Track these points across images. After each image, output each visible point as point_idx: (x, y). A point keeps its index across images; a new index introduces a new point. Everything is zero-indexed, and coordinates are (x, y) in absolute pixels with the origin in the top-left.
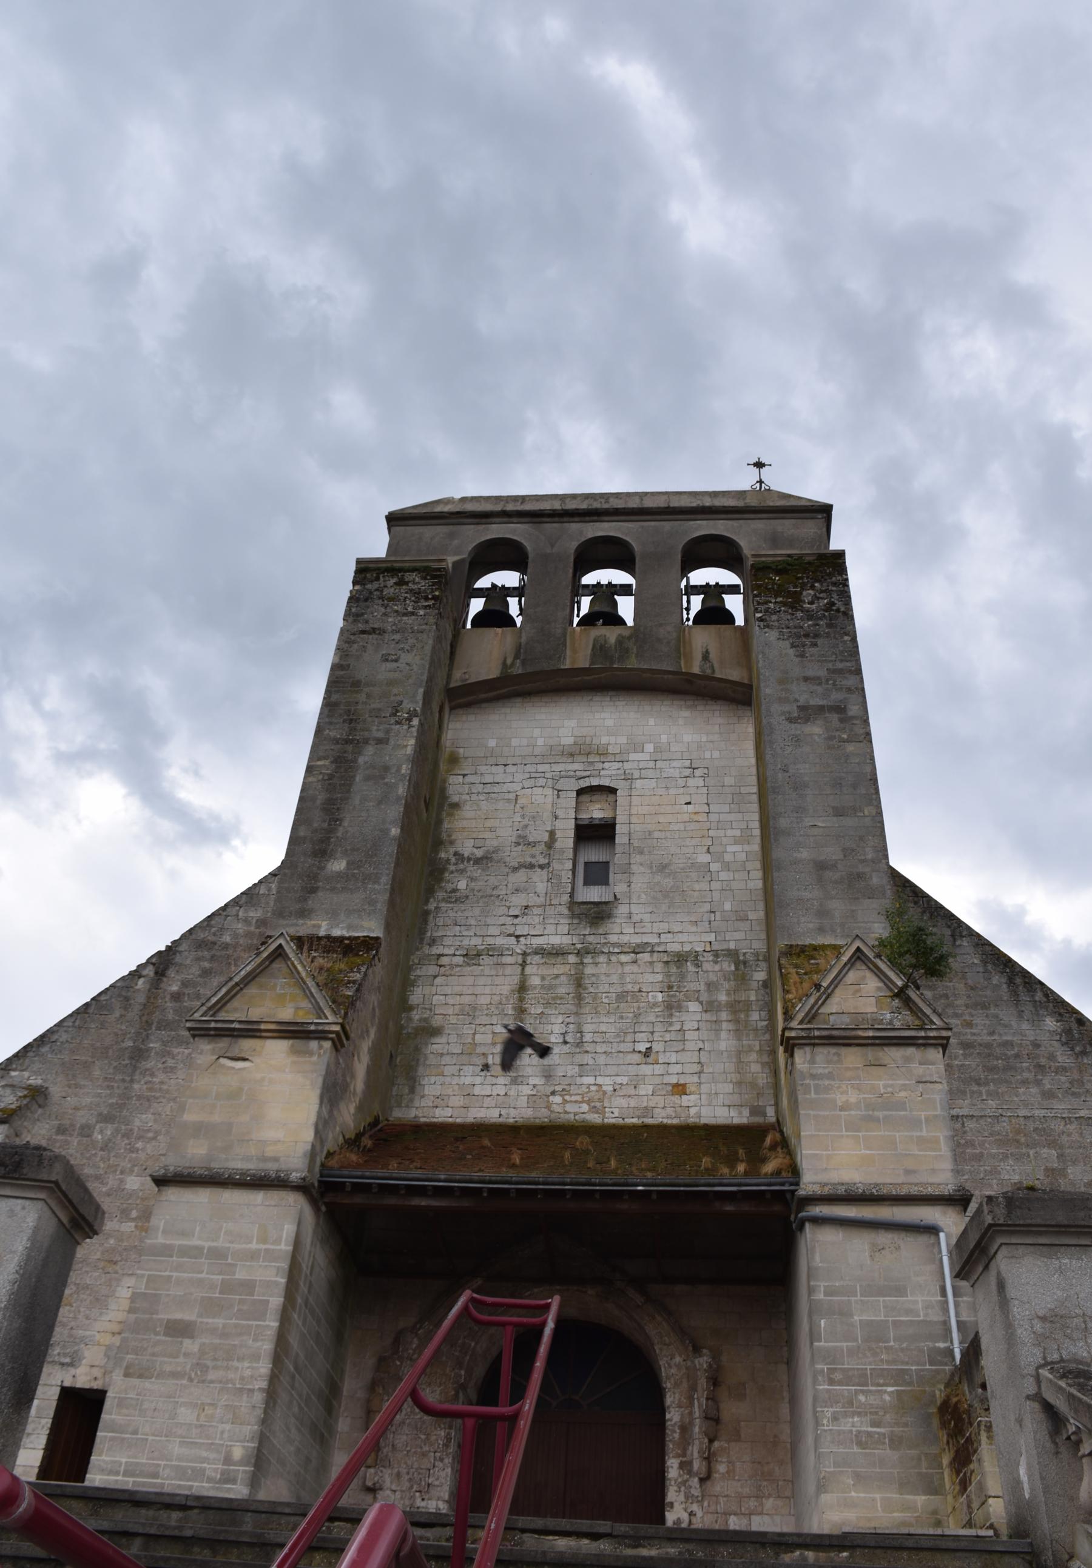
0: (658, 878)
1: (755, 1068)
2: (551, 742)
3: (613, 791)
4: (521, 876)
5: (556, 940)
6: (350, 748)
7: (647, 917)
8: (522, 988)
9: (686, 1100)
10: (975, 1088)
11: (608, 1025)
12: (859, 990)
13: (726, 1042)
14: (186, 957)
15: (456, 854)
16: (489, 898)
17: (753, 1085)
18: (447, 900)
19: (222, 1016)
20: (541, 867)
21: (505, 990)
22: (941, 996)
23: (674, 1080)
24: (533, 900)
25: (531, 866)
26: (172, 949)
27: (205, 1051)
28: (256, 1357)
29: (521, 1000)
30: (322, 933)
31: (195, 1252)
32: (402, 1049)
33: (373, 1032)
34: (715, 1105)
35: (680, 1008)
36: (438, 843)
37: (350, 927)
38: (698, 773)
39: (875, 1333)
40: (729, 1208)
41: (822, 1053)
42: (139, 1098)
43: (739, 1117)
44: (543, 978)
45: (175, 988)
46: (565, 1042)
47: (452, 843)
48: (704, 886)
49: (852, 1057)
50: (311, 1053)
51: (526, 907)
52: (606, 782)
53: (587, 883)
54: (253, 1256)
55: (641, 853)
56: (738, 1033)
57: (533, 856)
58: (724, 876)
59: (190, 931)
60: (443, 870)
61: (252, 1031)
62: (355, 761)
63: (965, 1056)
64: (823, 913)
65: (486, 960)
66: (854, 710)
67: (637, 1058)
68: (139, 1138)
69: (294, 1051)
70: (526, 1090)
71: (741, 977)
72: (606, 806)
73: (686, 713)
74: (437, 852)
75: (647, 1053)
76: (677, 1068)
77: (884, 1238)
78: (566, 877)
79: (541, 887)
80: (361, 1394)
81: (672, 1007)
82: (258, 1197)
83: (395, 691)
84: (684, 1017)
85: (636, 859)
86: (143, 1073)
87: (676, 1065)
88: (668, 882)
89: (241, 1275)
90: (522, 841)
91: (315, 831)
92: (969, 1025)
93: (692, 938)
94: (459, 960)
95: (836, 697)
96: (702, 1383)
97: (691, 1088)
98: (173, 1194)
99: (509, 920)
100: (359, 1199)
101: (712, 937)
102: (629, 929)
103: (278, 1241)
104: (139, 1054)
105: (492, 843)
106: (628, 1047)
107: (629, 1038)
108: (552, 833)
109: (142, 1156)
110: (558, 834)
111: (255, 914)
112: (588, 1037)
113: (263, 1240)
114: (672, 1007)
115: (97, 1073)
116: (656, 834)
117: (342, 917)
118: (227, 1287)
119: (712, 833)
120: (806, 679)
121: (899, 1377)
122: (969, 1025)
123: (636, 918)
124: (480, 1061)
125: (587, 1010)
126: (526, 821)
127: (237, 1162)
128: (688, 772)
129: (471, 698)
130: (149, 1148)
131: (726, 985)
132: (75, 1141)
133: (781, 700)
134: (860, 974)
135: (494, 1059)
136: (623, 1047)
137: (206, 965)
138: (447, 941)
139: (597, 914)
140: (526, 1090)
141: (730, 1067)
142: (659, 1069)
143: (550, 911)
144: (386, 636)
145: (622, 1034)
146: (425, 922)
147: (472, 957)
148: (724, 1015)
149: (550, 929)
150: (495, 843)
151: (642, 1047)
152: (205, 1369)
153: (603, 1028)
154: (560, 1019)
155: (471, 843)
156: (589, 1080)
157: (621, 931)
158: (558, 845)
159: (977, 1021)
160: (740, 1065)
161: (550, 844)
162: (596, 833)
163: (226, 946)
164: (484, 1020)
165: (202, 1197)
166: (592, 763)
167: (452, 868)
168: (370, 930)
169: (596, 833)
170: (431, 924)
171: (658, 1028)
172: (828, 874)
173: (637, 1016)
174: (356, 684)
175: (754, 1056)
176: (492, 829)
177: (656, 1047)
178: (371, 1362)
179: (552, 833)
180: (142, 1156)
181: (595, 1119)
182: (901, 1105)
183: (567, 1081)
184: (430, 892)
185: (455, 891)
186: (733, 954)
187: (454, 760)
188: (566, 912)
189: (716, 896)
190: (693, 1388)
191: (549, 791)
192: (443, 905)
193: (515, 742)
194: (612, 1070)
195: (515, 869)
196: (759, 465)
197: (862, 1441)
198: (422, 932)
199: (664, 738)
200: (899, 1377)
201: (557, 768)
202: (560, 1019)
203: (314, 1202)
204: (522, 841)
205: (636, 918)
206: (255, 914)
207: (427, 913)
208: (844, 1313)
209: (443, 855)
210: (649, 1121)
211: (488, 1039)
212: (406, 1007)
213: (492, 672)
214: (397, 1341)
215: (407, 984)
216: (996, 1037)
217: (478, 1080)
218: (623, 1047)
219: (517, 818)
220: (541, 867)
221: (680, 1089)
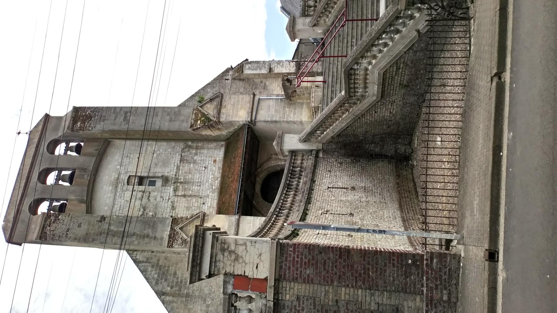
0: (159, 166)
1: (212, 145)
2: (110, 192)
3: (130, 176)
4: (152, 199)
5: (172, 190)
6: (110, 233)
7: (169, 168)
8: (184, 196)
9: (217, 160)
11: (197, 176)
13: (205, 151)
14: (160, 287)
16: (156, 207)
17: (216, 146)
21: (184, 199)
23: (212, 162)
24: (159, 195)
26: (157, 293)
34: (220, 154)
35: (195, 160)
37: (168, 226)
38: (129, 155)
39: (276, 111)
41: (221, 115)
42: (200, 293)
43: (223, 149)
45: (169, 288)
49: (223, 111)
52: (127, 178)
54: (254, 224)
56: (204, 148)
58: (161, 151)
62: (115, 231)
64: (183, 121)
65: (175, 204)
66: (128, 110)
67: (206, 170)
68: (211, 291)
70: (210, 194)
71: (190, 147)
73: (109, 158)
75: (205, 168)
76: (210, 162)
77: (260, 108)
79: (156, 193)
81: (195, 162)
82: (241, 225)
83: (92, 223)
86: (193, 293)
87: (209, 162)
88: (160, 163)
91: (136, 239)
95: (122, 113)
99: (164, 201)
101: (177, 154)
104: (188, 295)
106: (203, 172)
109: (216, 289)
111: (150, 269)
112: (199, 181)
114: (195, 162)
115: (192, 307)
120: (115, 119)
121: (284, 108)
124: (202, 205)
128: (128, 158)
130: (214, 287)
131: (191, 151)
132: (210, 309)
133: (121, 125)
137: (163, 281)
139: (166, 180)
140: (210, 194)
141: (211, 150)
142: (209, 165)
143: (163, 191)
144: (70, 227)
145: (199, 173)
147: (173, 208)
148: (199, 151)
151: (204, 169)
153: (198, 177)
154: (194, 187)
160: (211, 148)
162: (141, 181)
163: (158, 276)
164: (191, 204)
169: (141, 181)
172: (173, 119)
174: (87, 234)
175: (209, 146)
177: (204, 166)
180: (216, 289)
181: (219, 179)
182: (234, 103)
185: (152, 215)
186: (183, 149)
191: (126, 193)
193: (107, 202)
195: (149, 200)
196: (19, 133)
197: (295, 114)
199: (116, 163)
200: (284, 108)
206: (150, 269)
208: (273, 115)
211: (196, 203)
213: (84, 206)
217: (207, 205)
218: (203, 172)
220: (150, 194)
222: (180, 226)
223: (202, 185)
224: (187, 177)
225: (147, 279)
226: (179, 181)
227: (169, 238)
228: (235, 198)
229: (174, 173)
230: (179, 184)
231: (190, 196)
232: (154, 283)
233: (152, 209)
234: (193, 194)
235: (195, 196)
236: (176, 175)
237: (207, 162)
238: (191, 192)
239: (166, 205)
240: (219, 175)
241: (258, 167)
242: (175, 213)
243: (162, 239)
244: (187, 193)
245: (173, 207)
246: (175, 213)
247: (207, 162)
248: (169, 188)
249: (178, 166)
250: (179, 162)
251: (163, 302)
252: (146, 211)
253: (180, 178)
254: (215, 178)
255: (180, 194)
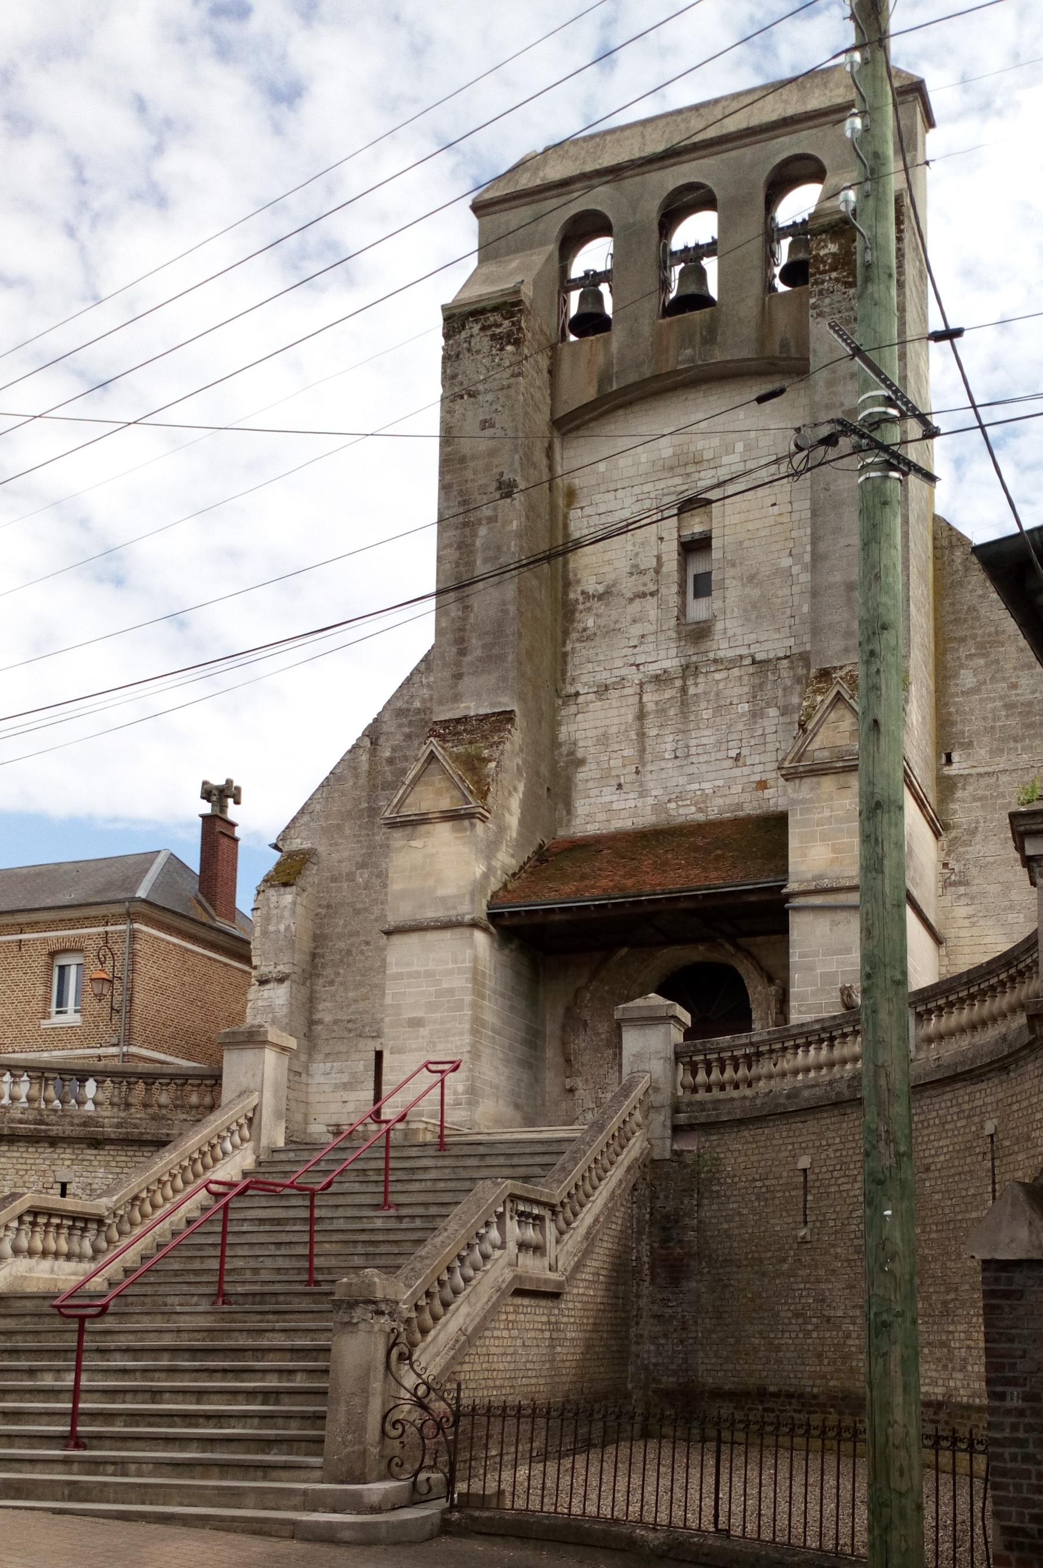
0: (747, 590)
5: (667, 664)
7: (739, 631)
8: (641, 716)
9: (768, 793)
10: (1012, 744)
12: (837, 727)
15: (583, 593)
16: (610, 632)
18: (579, 640)
19: (405, 811)
20: (652, 594)
21: (630, 718)
22: (992, 663)
23: (757, 778)
25: (643, 595)
27: (398, 838)
28: (462, 1034)
29: (642, 726)
30: (472, 714)
31: (416, 975)
32: (555, 781)
33: (521, 788)
36: (567, 584)
37: (492, 705)
40: (753, 898)
44: (657, 703)
46: (676, 757)
47: (578, 581)
48: (786, 591)
50: (465, 830)
51: (643, 636)
53: (697, 595)
54: (450, 972)
55: (733, 566)
57: (645, 585)
59: (389, 702)
60: (573, 612)
61: (422, 820)
63: (1007, 716)
65: (613, 694)
67: (730, 763)
69: (455, 830)
72: (705, 518)
74: (566, 593)
78: (674, 600)
79: (653, 614)
80: (558, 1033)
81: (756, 714)
82: (447, 934)
84: (766, 722)
85: (730, 572)
88: (756, 593)
89: (445, 985)
90: (636, 571)
92: (1014, 686)
93: (776, 645)
94: (592, 697)
96: (773, 1004)
97: (771, 783)
98: (396, 939)
100: (515, 921)
102: (724, 645)
103: (464, 961)
105: (610, 577)
107: (724, 746)
108: (659, 558)
110: (665, 558)
112: (693, 751)
113: (455, 962)
114: (756, 714)
116: (746, 544)
117: (484, 696)
118: (439, 994)
119: (794, 534)
122: (1014, 686)
123: (730, 633)
125: (692, 726)
126: (637, 549)
127: (431, 913)
129: (578, 422)
134: (841, 712)
135: (628, 776)
136: (720, 755)
138: (584, 679)
139: (698, 634)
142: (746, 770)
143: (662, 637)
146: (565, 663)
147: (603, 690)
149: (663, 654)
150: (613, 577)
151: (733, 753)
152: (434, 1044)
153: (704, 741)
154: (671, 738)
155: (593, 580)
156: (696, 786)
157: (721, 647)
158: (664, 570)
159: (1023, 682)
161: (657, 571)
163: (418, 711)
165: (414, 939)
166: (688, 475)
167: (581, 607)
168: (505, 705)
170: (570, 667)
171: (745, 735)
173: (729, 727)
176: (610, 562)
177: (745, 752)
178: (560, 1011)
179: (659, 558)
183: (679, 789)
184: (566, 633)
187: (571, 495)
188: (674, 635)
189: (796, 598)
190: (769, 1008)
192: (577, 645)
194: (713, 775)
195: (631, 600)
198: (564, 673)
201: (661, 485)
202: (671, 738)
203: (485, 930)
204: (636, 571)
205: (730, 633)
207: (565, 655)
209: (572, 596)
210: (741, 814)
211: (619, 762)
212: (555, 743)
214: (576, 996)
215: (555, 725)
216: (1037, 695)
218: (720, 755)
219: (630, 548)
220: (652, 594)
221: (762, 785)
222: (439, 752)
223: (677, 762)
224: (703, 705)
225: (408, 680)
226: (690, 682)
227: (458, 721)
228: (560, 894)
229: (721, 654)
230: (678, 683)
231: (642, 735)
232: (400, 704)
233: (602, 622)
234: (649, 742)
235: (642, 751)
236: (715, 661)
237: (756, 759)
238: (653, 732)
239: (618, 663)
240: (713, 814)
241: (743, 941)
242: (587, 703)
243: (456, 698)
244: (651, 721)
245: (607, 688)
246: (587, 703)
247: (756, 759)
248: (673, 652)
249: (741, 657)
250: (759, 657)
251: (355, 748)
252: (596, 604)
253: (701, 679)
254: (702, 801)
255: (646, 698)
